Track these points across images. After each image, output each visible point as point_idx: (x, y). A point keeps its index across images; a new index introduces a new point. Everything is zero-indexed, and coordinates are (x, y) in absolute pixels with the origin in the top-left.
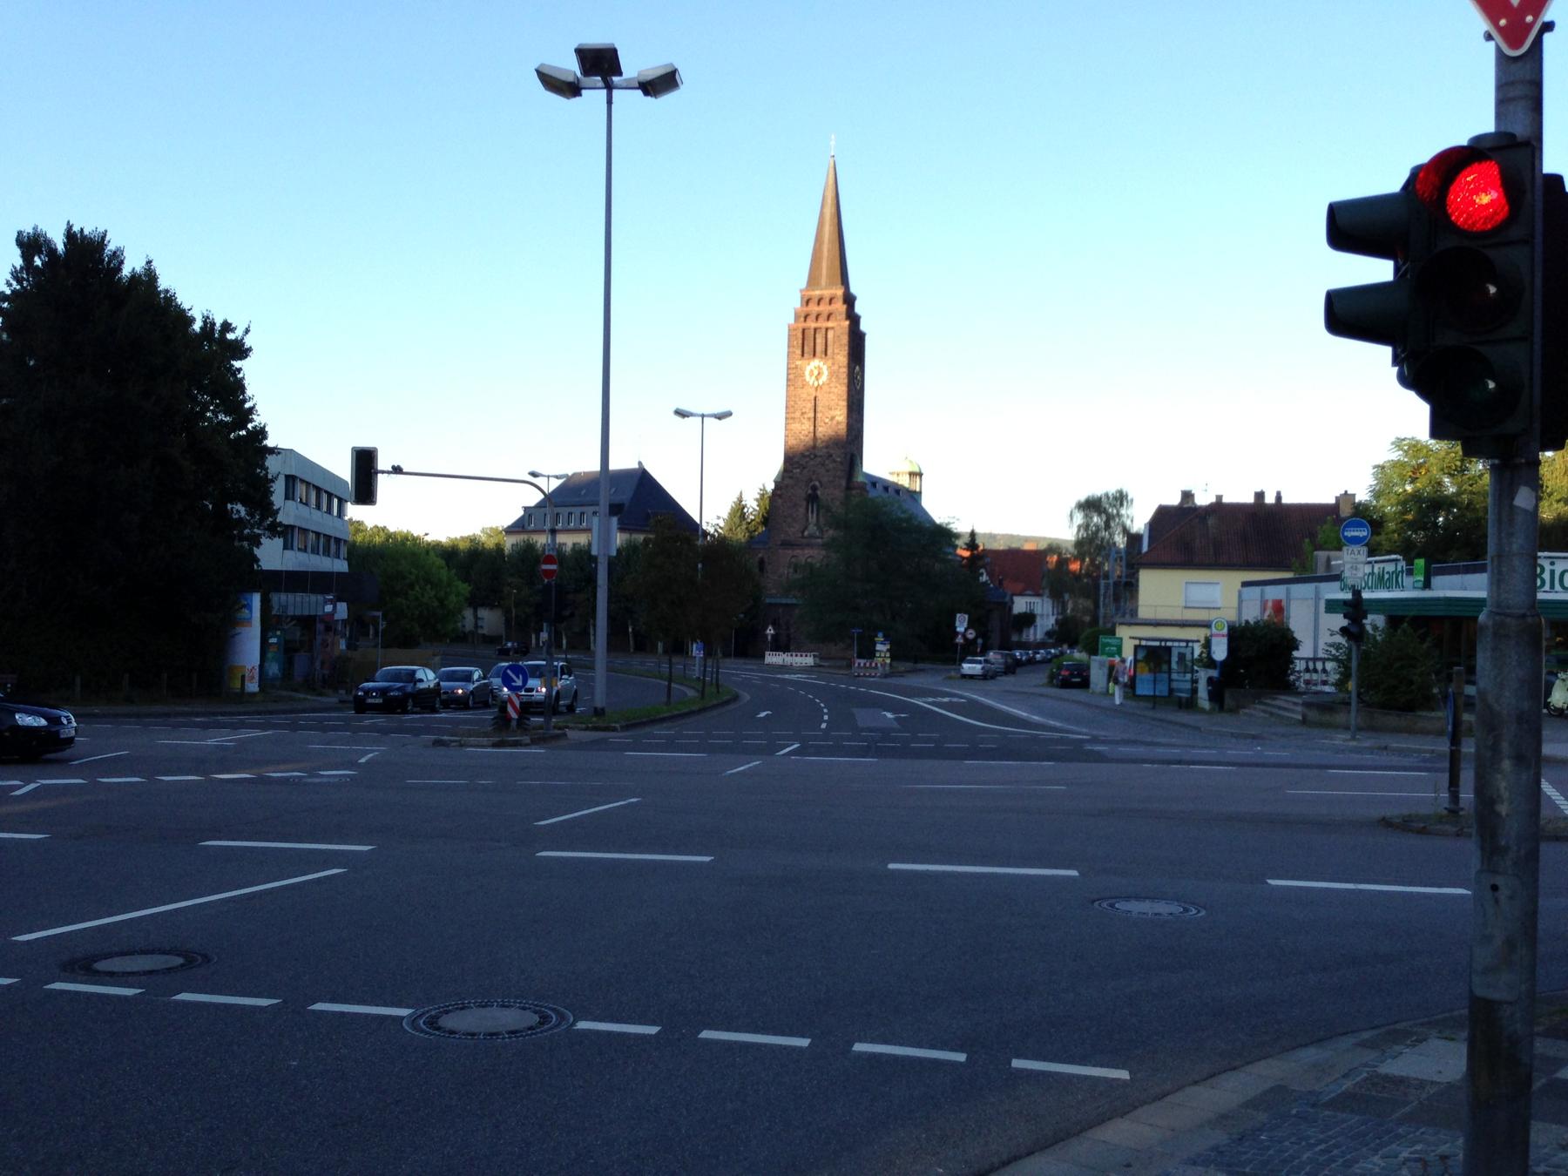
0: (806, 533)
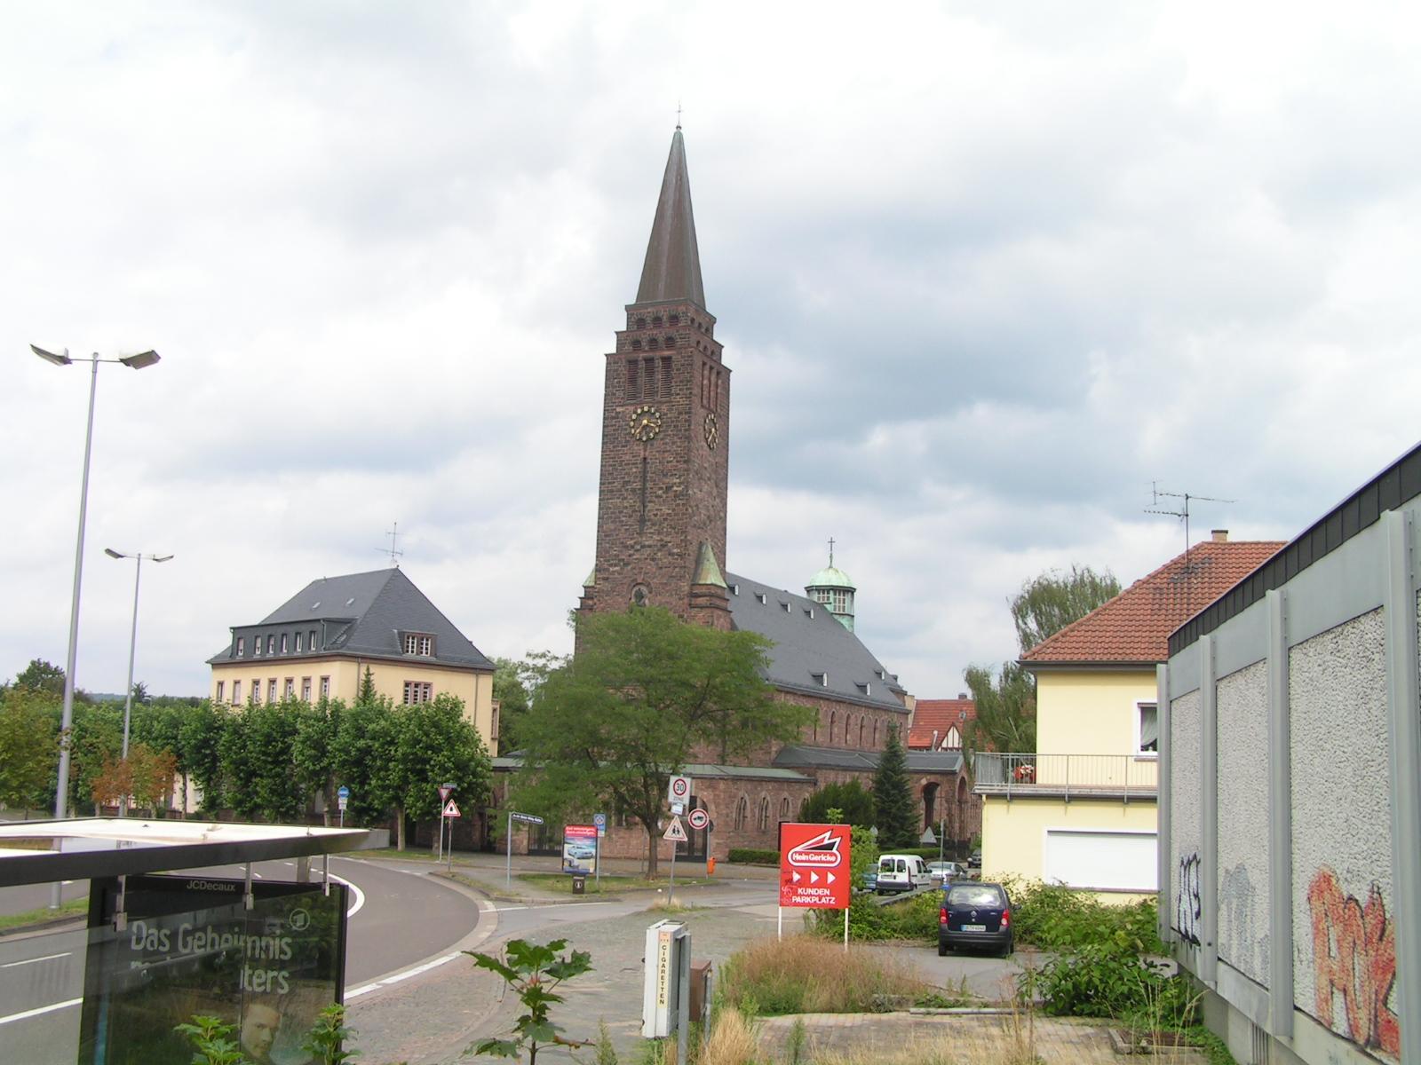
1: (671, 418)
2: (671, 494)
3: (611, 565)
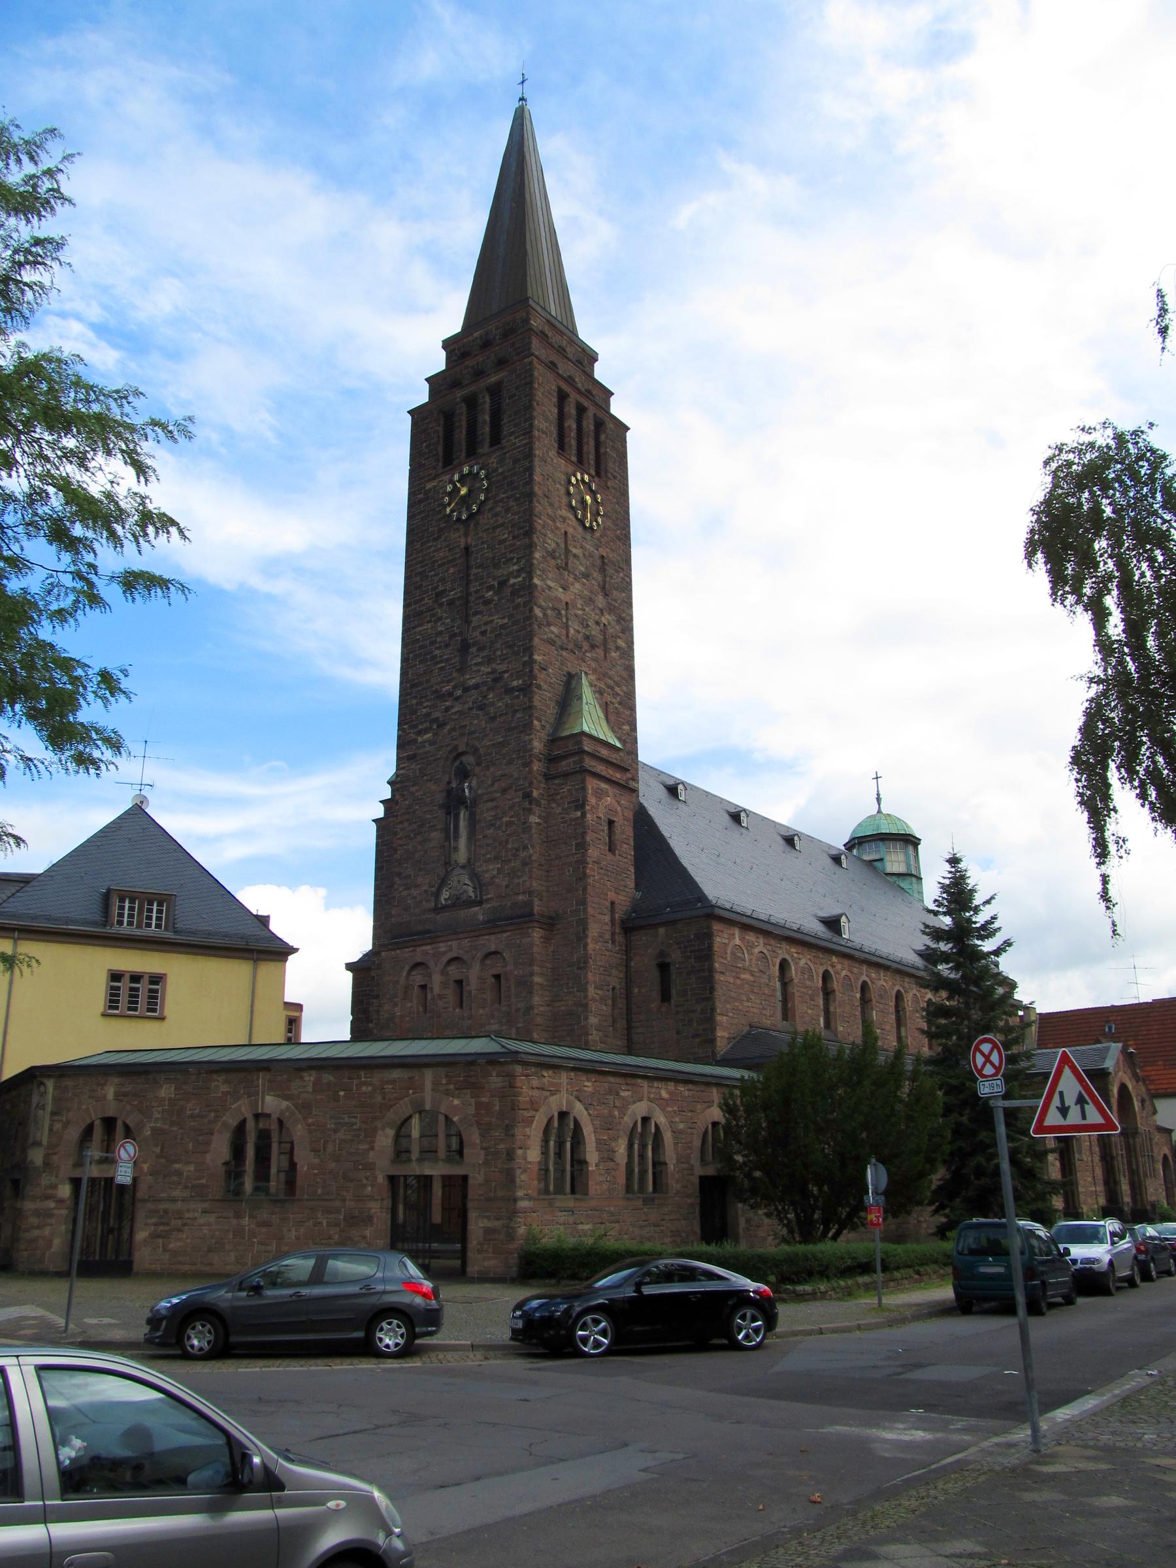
0: (445, 895)
1: (502, 473)
2: (507, 591)
3: (419, 733)
